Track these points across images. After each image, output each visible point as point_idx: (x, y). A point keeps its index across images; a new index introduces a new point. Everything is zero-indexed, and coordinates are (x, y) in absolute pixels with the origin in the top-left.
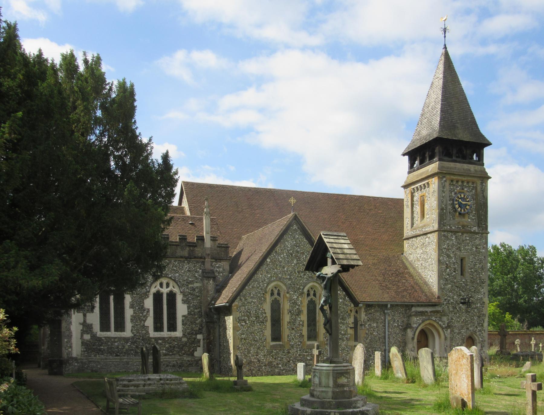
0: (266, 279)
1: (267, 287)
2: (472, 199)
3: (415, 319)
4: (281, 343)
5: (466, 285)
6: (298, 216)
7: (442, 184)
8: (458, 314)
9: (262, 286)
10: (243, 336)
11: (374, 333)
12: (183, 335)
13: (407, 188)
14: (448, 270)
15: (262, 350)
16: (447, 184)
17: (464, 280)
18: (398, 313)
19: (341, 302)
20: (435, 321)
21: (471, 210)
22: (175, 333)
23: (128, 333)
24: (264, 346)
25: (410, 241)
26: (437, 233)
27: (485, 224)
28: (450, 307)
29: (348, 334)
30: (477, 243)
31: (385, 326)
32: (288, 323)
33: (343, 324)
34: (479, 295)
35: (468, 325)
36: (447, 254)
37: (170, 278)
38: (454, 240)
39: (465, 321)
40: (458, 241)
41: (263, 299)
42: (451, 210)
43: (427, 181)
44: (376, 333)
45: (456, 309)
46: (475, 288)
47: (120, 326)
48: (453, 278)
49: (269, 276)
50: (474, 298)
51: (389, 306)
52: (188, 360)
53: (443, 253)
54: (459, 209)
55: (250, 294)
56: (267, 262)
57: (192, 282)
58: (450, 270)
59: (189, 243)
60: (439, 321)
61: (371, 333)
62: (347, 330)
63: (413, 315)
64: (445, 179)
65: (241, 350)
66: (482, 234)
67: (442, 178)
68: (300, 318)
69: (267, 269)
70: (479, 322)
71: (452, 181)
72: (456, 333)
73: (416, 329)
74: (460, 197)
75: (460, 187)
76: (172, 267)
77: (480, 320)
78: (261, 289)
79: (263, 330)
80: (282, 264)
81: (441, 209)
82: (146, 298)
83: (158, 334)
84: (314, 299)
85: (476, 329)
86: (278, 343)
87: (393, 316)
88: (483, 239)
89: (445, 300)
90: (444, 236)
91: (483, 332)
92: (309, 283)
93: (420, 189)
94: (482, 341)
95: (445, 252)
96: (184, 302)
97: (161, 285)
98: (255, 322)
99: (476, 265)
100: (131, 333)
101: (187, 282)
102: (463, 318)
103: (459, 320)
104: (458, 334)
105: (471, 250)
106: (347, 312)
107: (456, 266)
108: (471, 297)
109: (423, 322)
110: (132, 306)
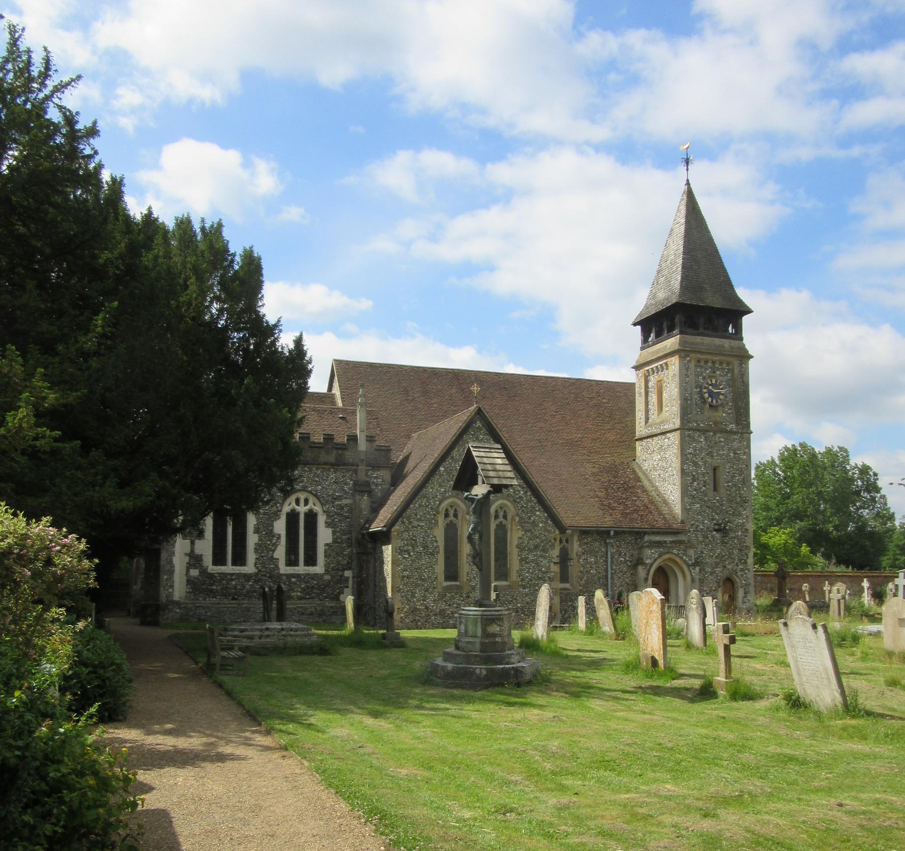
0: (438, 494)
1: (439, 505)
3: (648, 552)
4: (458, 583)
6: (482, 409)
7: (685, 365)
9: (432, 504)
10: (406, 573)
11: (592, 571)
12: (326, 570)
13: (639, 370)
14: (696, 483)
15: (431, 593)
16: (692, 365)
17: (718, 498)
18: (625, 543)
19: (542, 527)
20: (677, 555)
21: (726, 401)
22: (314, 568)
23: (249, 568)
25: (644, 443)
26: (678, 432)
27: (745, 421)
28: (699, 536)
29: (551, 572)
31: (606, 561)
32: (467, 555)
33: (545, 557)
34: (740, 519)
35: (725, 561)
37: (310, 492)
41: (433, 521)
43: (665, 361)
44: (595, 572)
45: (708, 538)
46: (734, 509)
47: (240, 558)
49: (443, 490)
51: (612, 533)
52: (331, 607)
54: (710, 400)
55: (416, 515)
56: (440, 471)
57: (339, 498)
58: (698, 484)
59: (337, 444)
60: (684, 555)
61: (587, 571)
62: (550, 565)
63: (646, 546)
65: (403, 592)
66: (742, 434)
67: (685, 357)
69: (440, 480)
76: (314, 477)
77: (742, 555)
78: (432, 508)
79: (433, 564)
81: (684, 399)
82: (276, 519)
83: (291, 570)
84: (504, 523)
88: (744, 441)
89: (692, 525)
90: (689, 436)
92: (497, 500)
93: (656, 371)
94: (746, 585)
96: (328, 525)
97: (297, 502)
98: (423, 554)
99: (736, 477)
100: (254, 568)
101: (333, 498)
104: (711, 575)
106: (550, 541)
107: (707, 478)
108: (728, 522)
109: (660, 556)
110: (257, 531)
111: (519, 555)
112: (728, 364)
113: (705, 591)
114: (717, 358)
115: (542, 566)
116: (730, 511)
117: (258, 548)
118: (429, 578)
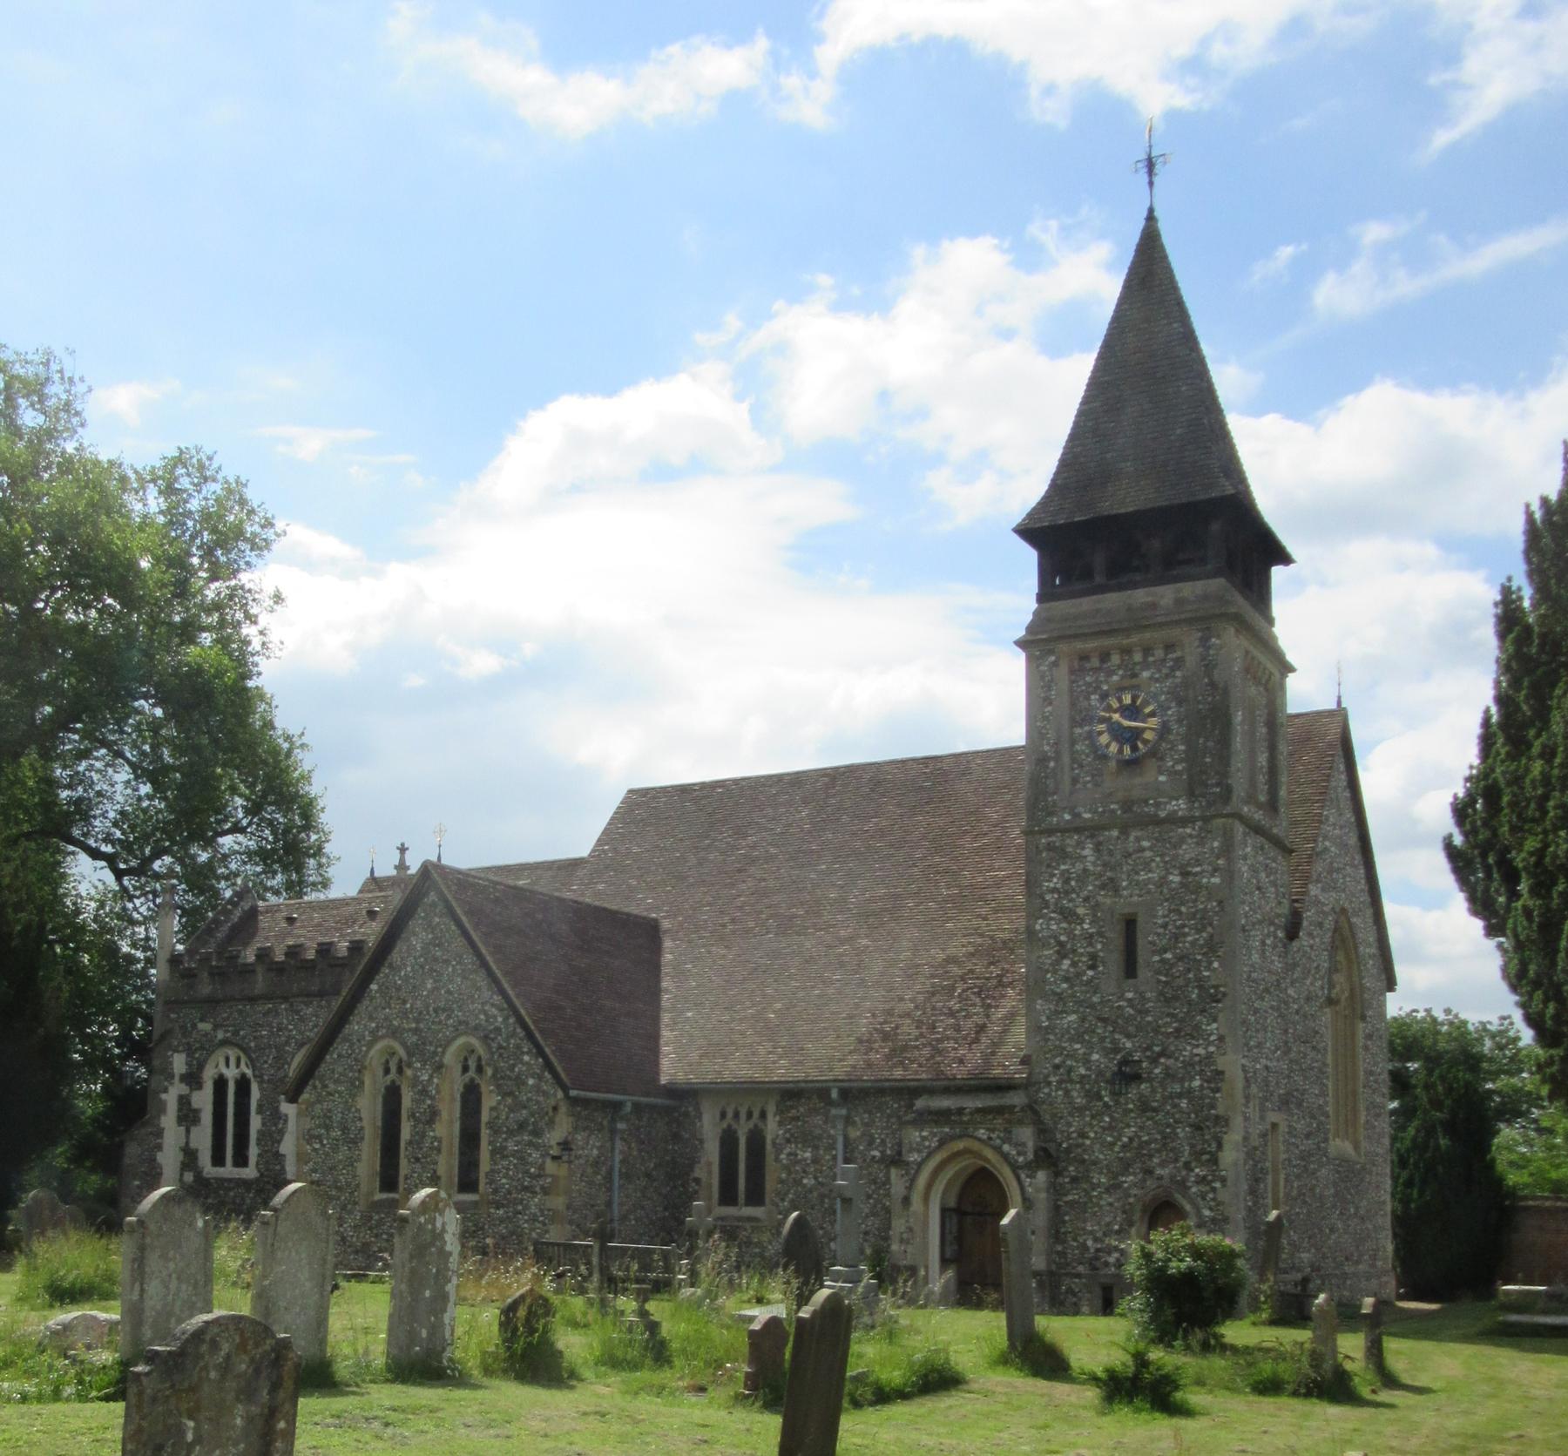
2: (1173, 704)
3: (915, 1135)
7: (1042, 678)
8: (1107, 1119)
11: (805, 1181)
14: (1066, 963)
16: (1062, 673)
17: (1130, 995)
23: (250, 1172)
24: (356, 1203)
28: (1075, 1094)
33: (537, 1147)
34: (1197, 1046)
35: (1151, 1156)
39: (1135, 1144)
42: (1087, 756)
44: (813, 1182)
45: (1100, 1098)
46: (1182, 1021)
48: (1087, 992)
49: (374, 1025)
50: (1177, 1059)
51: (834, 1094)
53: (1047, 908)
54: (1114, 748)
58: (1074, 964)
61: (795, 1180)
62: (544, 1162)
63: (909, 1123)
64: (1053, 658)
66: (1206, 820)
68: (434, 1131)
70: (1199, 1147)
71: (1084, 657)
72: (1099, 1185)
73: (918, 1171)
74: (1115, 705)
75: (1121, 672)
77: (1205, 1141)
78: (356, 1060)
80: (403, 994)
85: (1184, 1173)
86: (391, 1195)
87: (866, 1125)
88: (1214, 839)
89: (1057, 1067)
91: (1217, 1185)
92: (454, 1039)
95: (1056, 904)
99: (1185, 935)
103: (1109, 1139)
104: (1107, 1190)
105: (1161, 885)
108: (1162, 1054)
109: (942, 1143)
111: (490, 1143)
113: (1091, 1233)
114: (1135, 639)
115: (532, 1165)
117: (262, 1135)
118: (348, 1184)
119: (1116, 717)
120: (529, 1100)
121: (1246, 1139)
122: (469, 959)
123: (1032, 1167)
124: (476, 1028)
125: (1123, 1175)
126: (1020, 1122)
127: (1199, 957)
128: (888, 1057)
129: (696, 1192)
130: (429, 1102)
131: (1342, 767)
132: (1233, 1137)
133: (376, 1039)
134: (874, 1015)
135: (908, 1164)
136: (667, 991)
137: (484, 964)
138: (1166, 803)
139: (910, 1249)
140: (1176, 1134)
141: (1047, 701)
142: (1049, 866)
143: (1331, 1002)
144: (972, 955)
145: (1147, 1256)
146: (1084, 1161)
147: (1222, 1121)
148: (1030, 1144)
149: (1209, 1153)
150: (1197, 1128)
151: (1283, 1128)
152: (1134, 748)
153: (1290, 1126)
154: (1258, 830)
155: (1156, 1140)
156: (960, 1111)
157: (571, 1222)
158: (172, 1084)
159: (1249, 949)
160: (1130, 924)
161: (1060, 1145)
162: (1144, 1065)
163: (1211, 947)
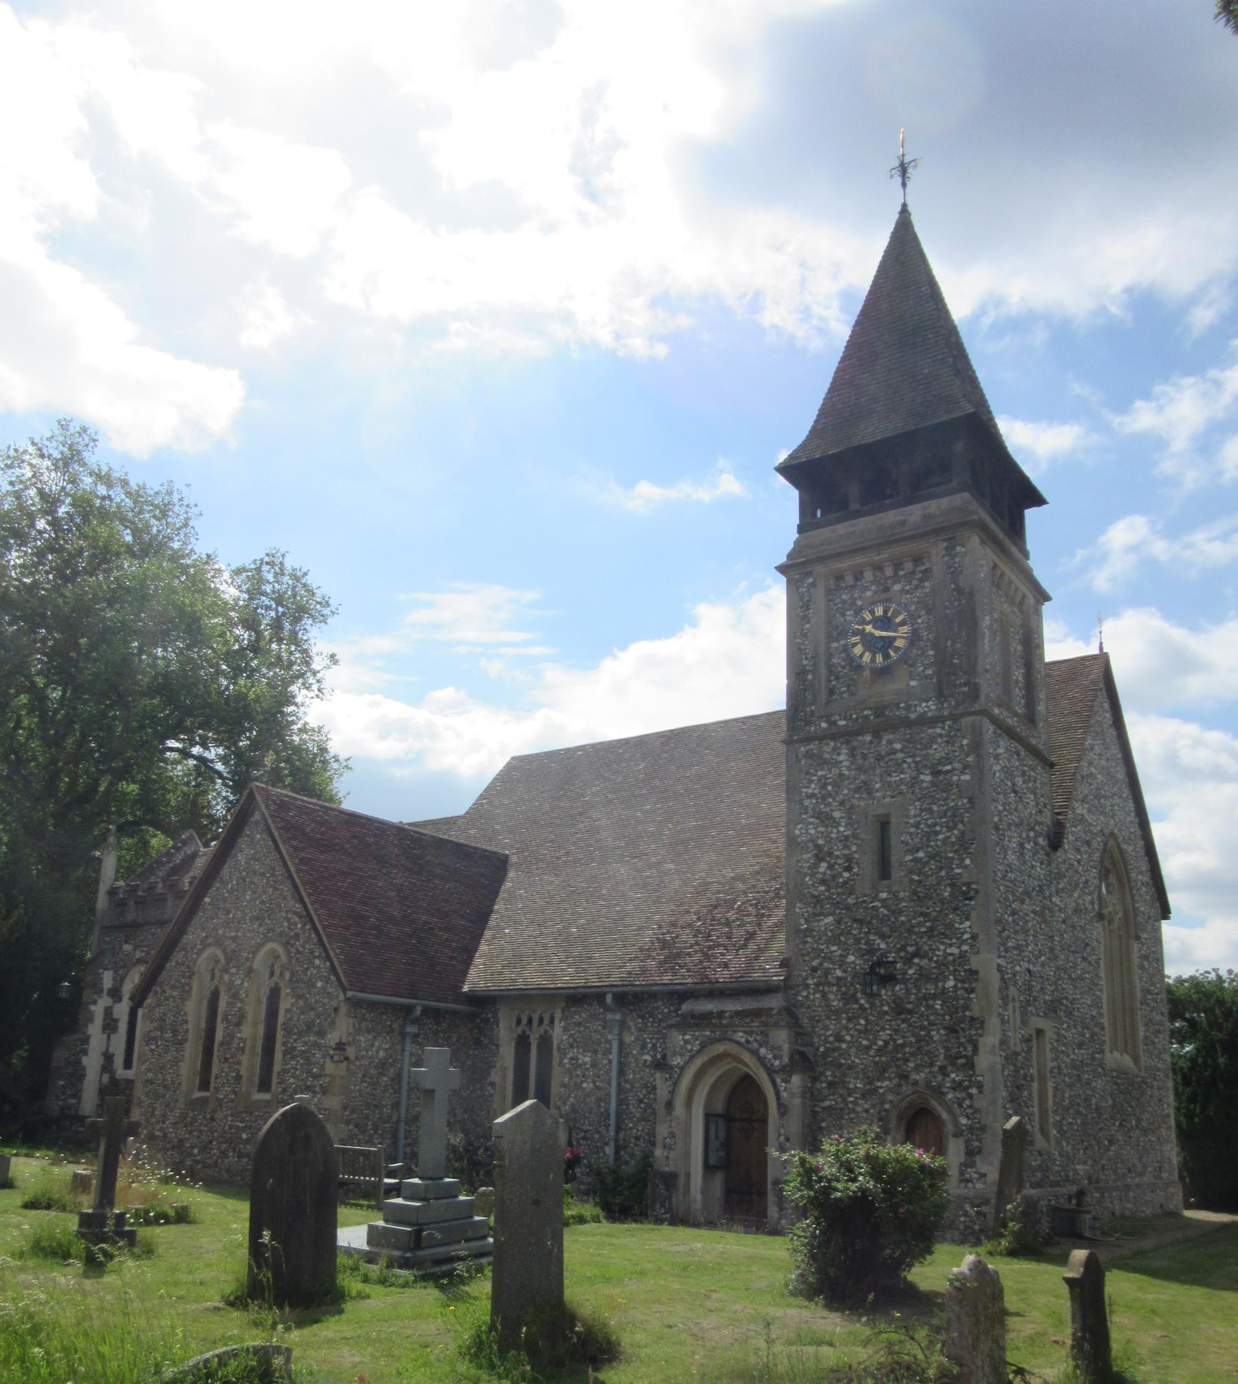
1: (197, 959)
2: (923, 613)
5: (893, 912)
7: (801, 598)
8: (862, 1022)
11: (585, 1085)
14: (824, 865)
17: (884, 895)
18: (653, 1022)
20: (745, 1046)
28: (831, 997)
30: (938, 756)
34: (951, 945)
35: (906, 1060)
36: (821, 813)
38: (844, 764)
39: (890, 1048)
40: (861, 762)
42: (844, 668)
44: (591, 1085)
45: (856, 1001)
48: (843, 894)
49: (204, 934)
50: (931, 960)
53: (806, 813)
54: (867, 657)
58: (831, 867)
60: (761, 1046)
62: (324, 1063)
64: (811, 580)
66: (955, 718)
68: (241, 1032)
70: (954, 1051)
73: (680, 1075)
74: (868, 617)
75: (874, 588)
81: (798, 674)
85: (940, 1078)
87: (640, 1030)
88: (964, 737)
89: (814, 970)
90: (808, 755)
91: (974, 1091)
92: (262, 945)
94: (971, 1129)
95: (814, 809)
99: (937, 833)
102: (884, 1035)
103: (865, 1042)
104: (863, 1096)
105: (913, 785)
108: (916, 954)
109: (703, 1046)
112: (917, 560)
116: (919, 924)
118: (173, 1083)
119: (869, 628)
120: (316, 1001)
121: (1004, 1042)
122: (280, 871)
123: (787, 1071)
124: (281, 934)
125: (878, 1081)
126: (776, 1025)
127: (950, 855)
128: (661, 964)
129: (491, 1096)
130: (239, 1005)
131: (1106, 706)
132: (989, 1040)
133: (204, 947)
134: (660, 927)
135: (671, 1067)
136: (498, 912)
137: (290, 877)
138: (916, 706)
139: (672, 1155)
140: (931, 1037)
141: (805, 619)
142: (807, 773)
143: (1101, 917)
144: (758, 873)
145: (809, 1173)
146: (841, 1065)
147: (978, 1023)
148: (786, 1047)
149: (965, 1057)
150: (952, 1030)
151: (1050, 1034)
152: (886, 656)
153: (1058, 1034)
154: (1010, 733)
155: (910, 1044)
156: (721, 1014)
157: (348, 1123)
158: (101, 997)
159: (1005, 850)
160: (884, 826)
161: (818, 1049)
162: (898, 966)
163: (963, 844)
